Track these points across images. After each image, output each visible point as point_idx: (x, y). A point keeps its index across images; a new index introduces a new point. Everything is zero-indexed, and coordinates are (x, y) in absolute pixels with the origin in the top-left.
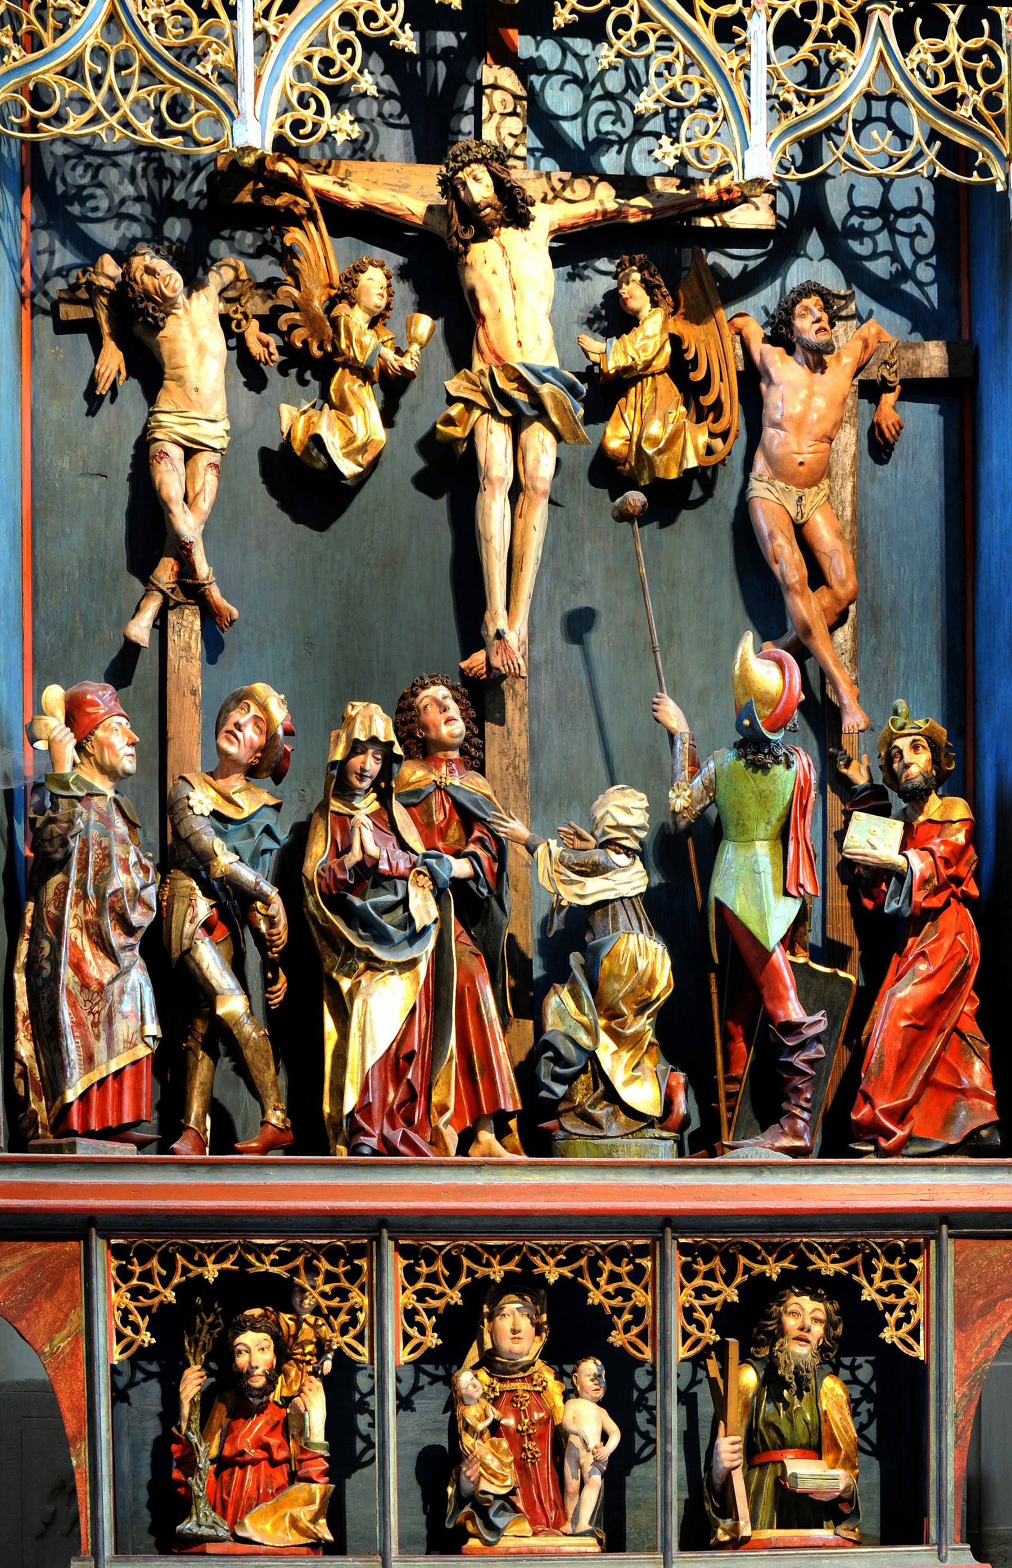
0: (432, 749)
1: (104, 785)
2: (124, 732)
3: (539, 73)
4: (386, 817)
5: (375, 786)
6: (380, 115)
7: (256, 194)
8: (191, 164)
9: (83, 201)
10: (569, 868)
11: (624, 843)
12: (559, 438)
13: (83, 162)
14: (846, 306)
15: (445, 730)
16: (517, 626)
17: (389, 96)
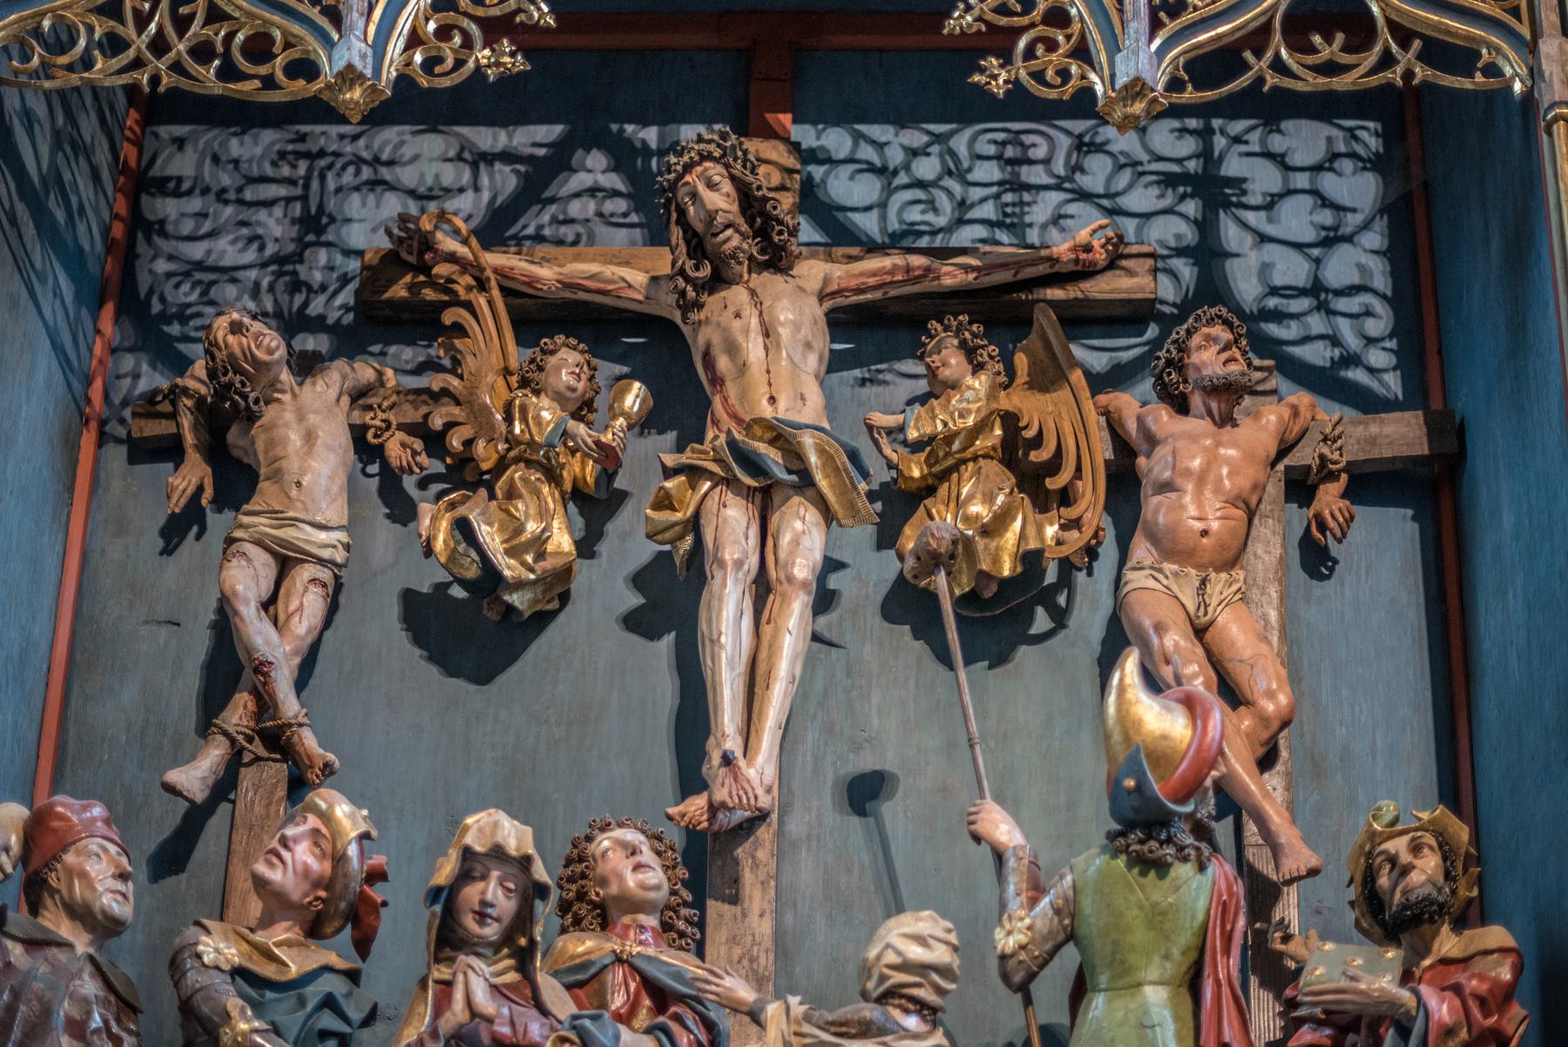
0: (613, 912)
1: (65, 929)
2: (111, 860)
3: (821, 162)
4: (528, 992)
5: (507, 939)
6: (600, 214)
7: (412, 288)
8: (335, 275)
9: (183, 319)
10: (820, 1028)
11: (915, 992)
12: (828, 515)
13: (192, 279)
14: (1264, 380)
15: (631, 880)
16: (760, 759)
17: (615, 194)
